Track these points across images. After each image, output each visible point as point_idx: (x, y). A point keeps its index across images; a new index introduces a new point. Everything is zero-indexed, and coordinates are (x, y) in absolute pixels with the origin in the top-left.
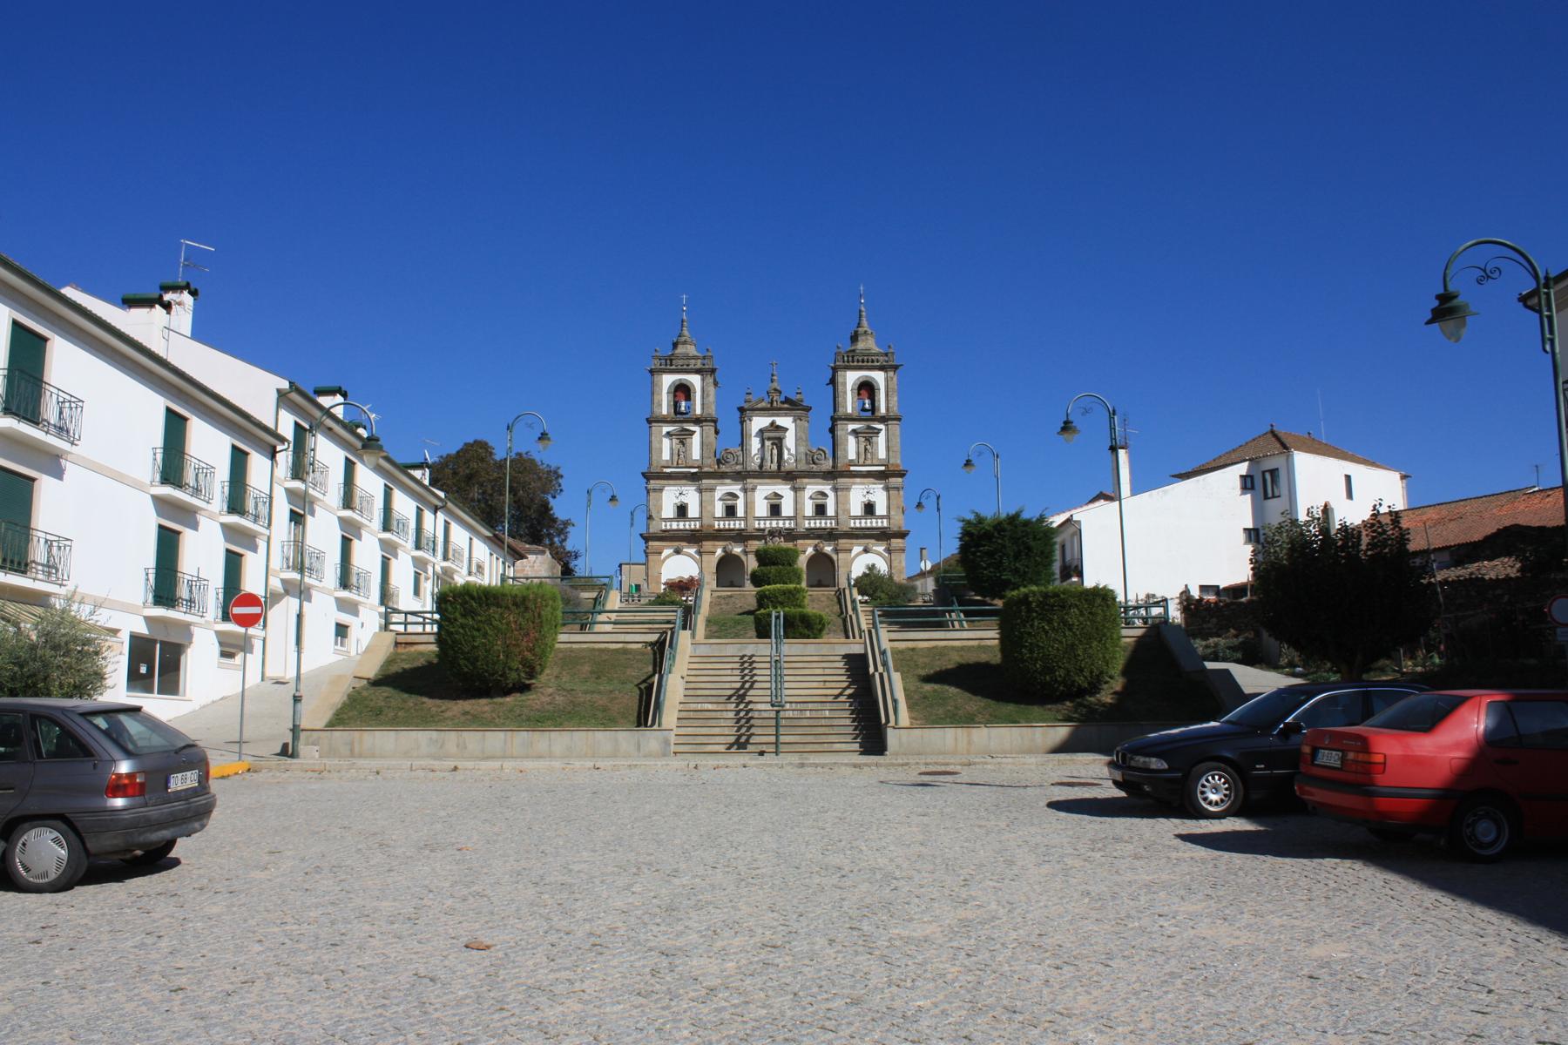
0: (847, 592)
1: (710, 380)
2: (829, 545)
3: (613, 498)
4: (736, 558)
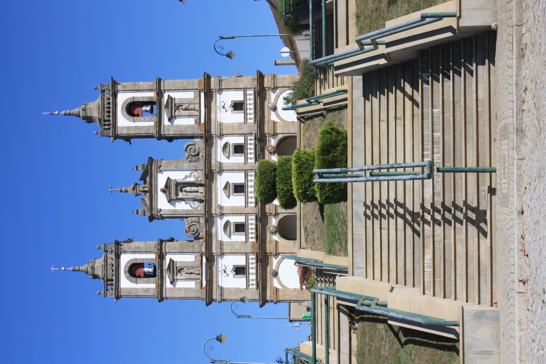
0: (301, 110)
1: (125, 246)
2: (270, 141)
3: (219, 339)
4: (281, 222)
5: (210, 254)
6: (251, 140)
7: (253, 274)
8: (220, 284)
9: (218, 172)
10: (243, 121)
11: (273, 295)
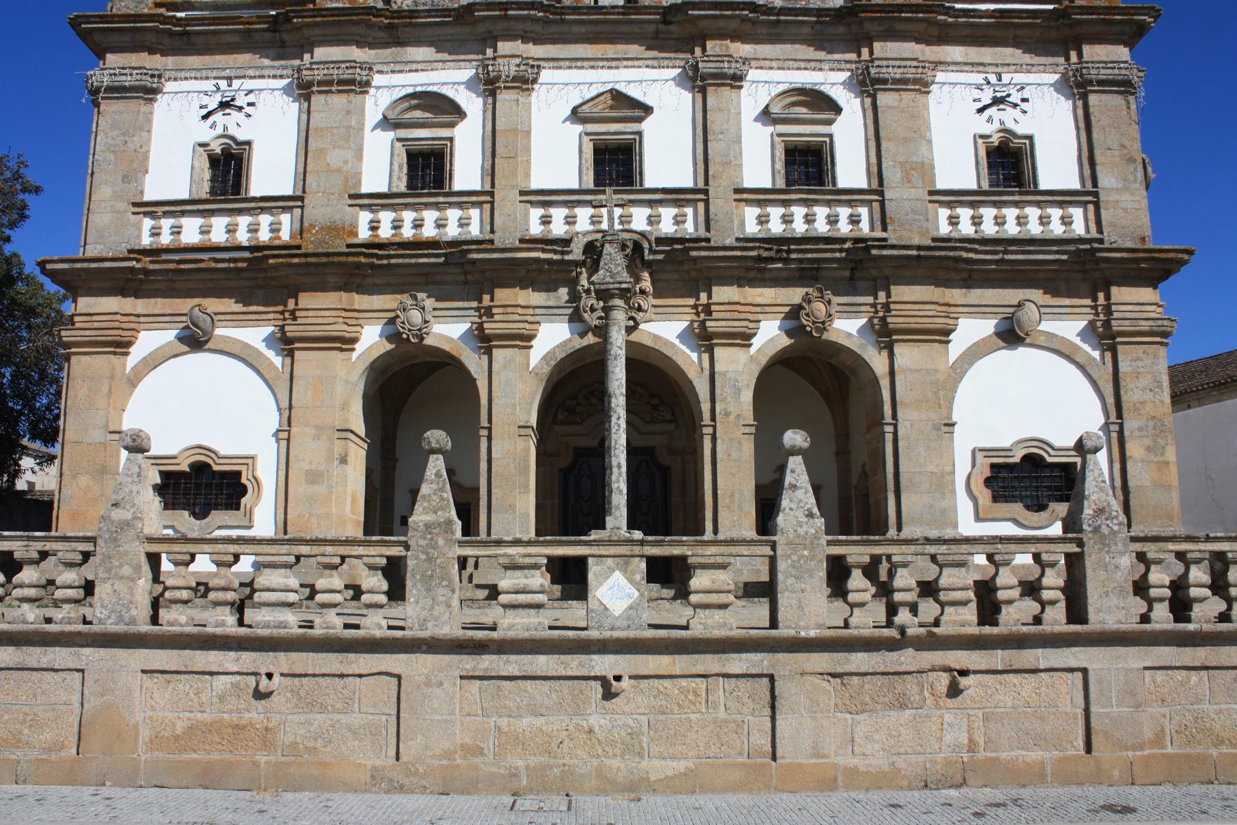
2: (851, 311)
5: (306, 32)
6: (854, 220)
7: (205, 231)
8: (170, 86)
9: (695, 67)
10: (941, 185)
11: (96, 325)
